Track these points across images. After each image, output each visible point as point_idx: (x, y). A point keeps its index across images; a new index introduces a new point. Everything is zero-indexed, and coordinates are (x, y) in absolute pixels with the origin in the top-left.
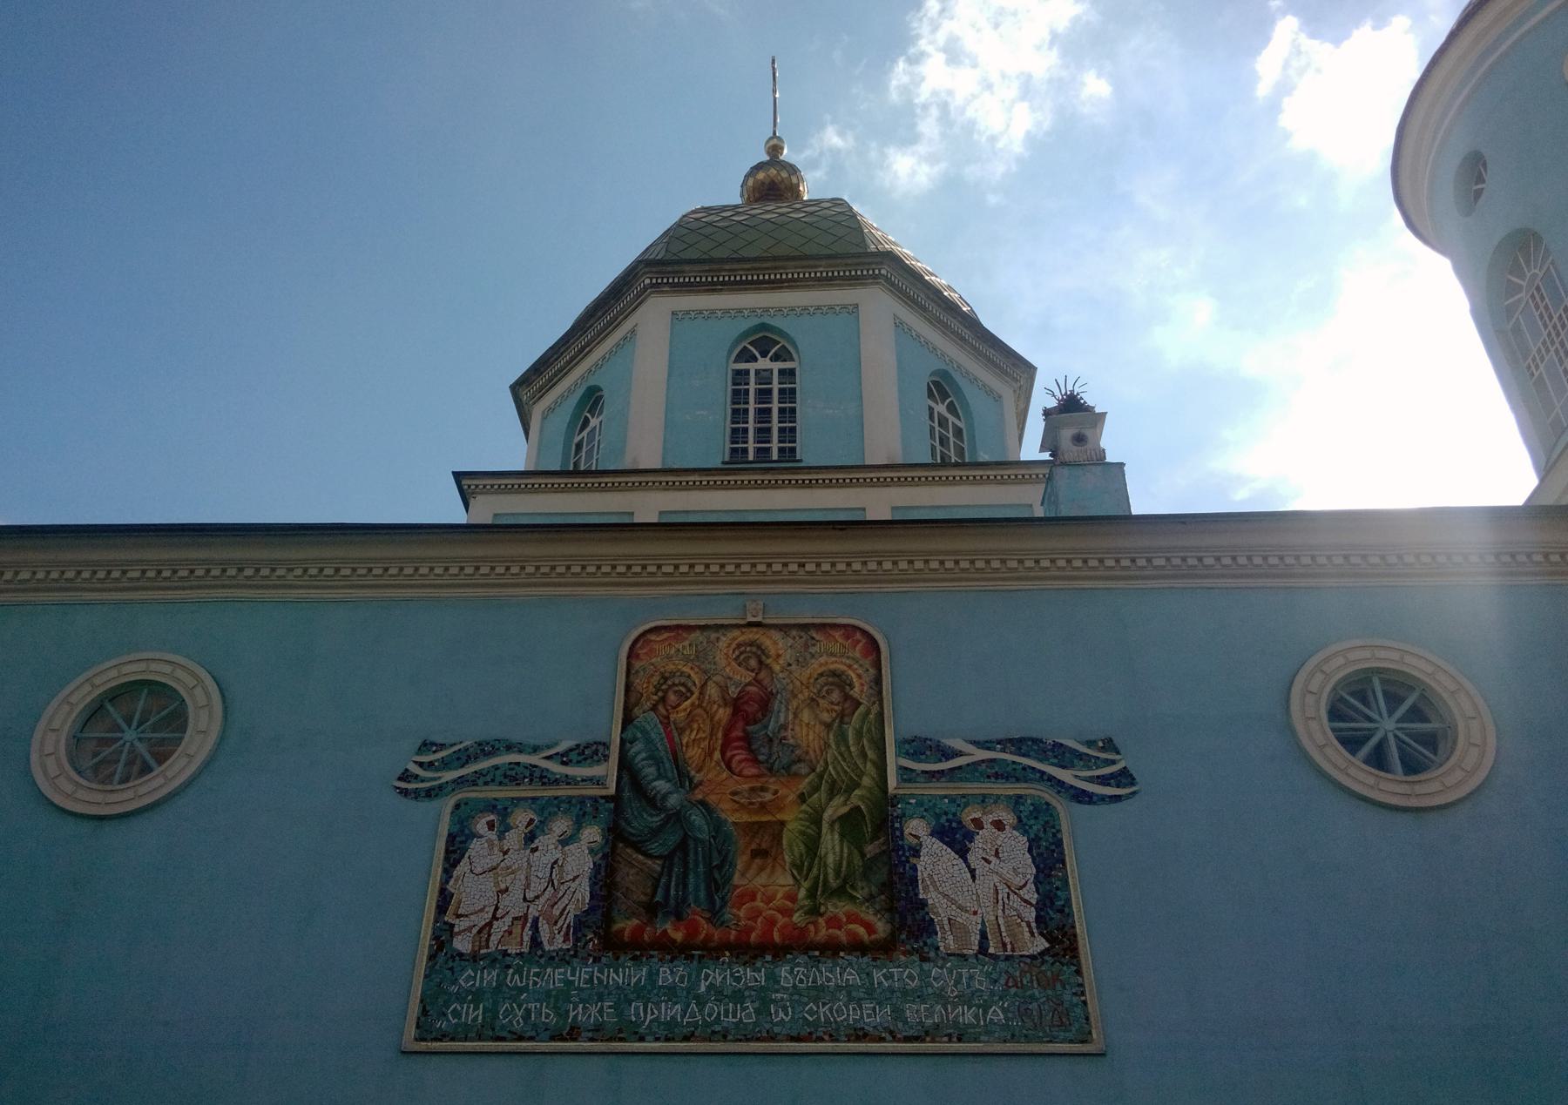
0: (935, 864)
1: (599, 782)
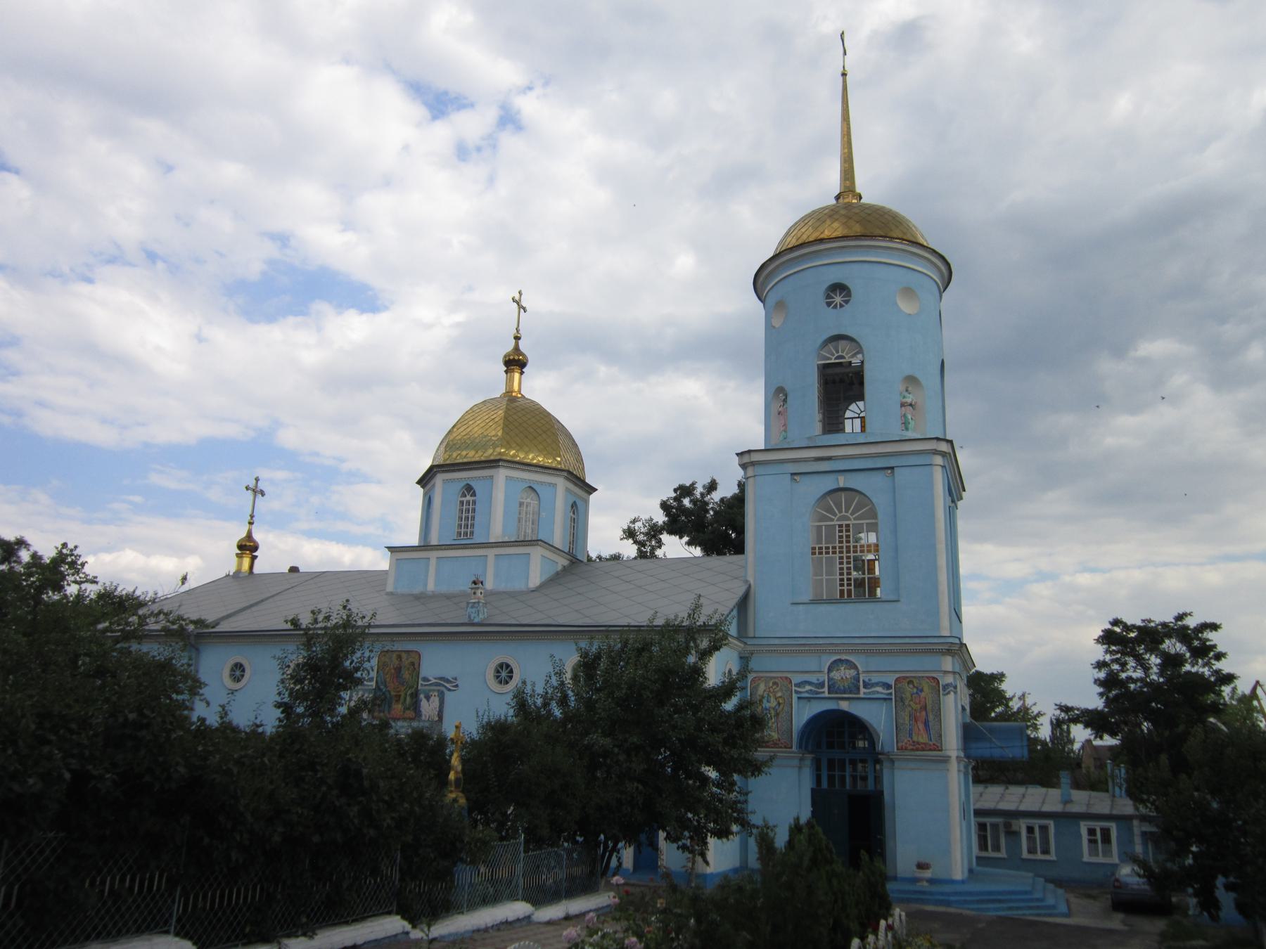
0: (424, 703)
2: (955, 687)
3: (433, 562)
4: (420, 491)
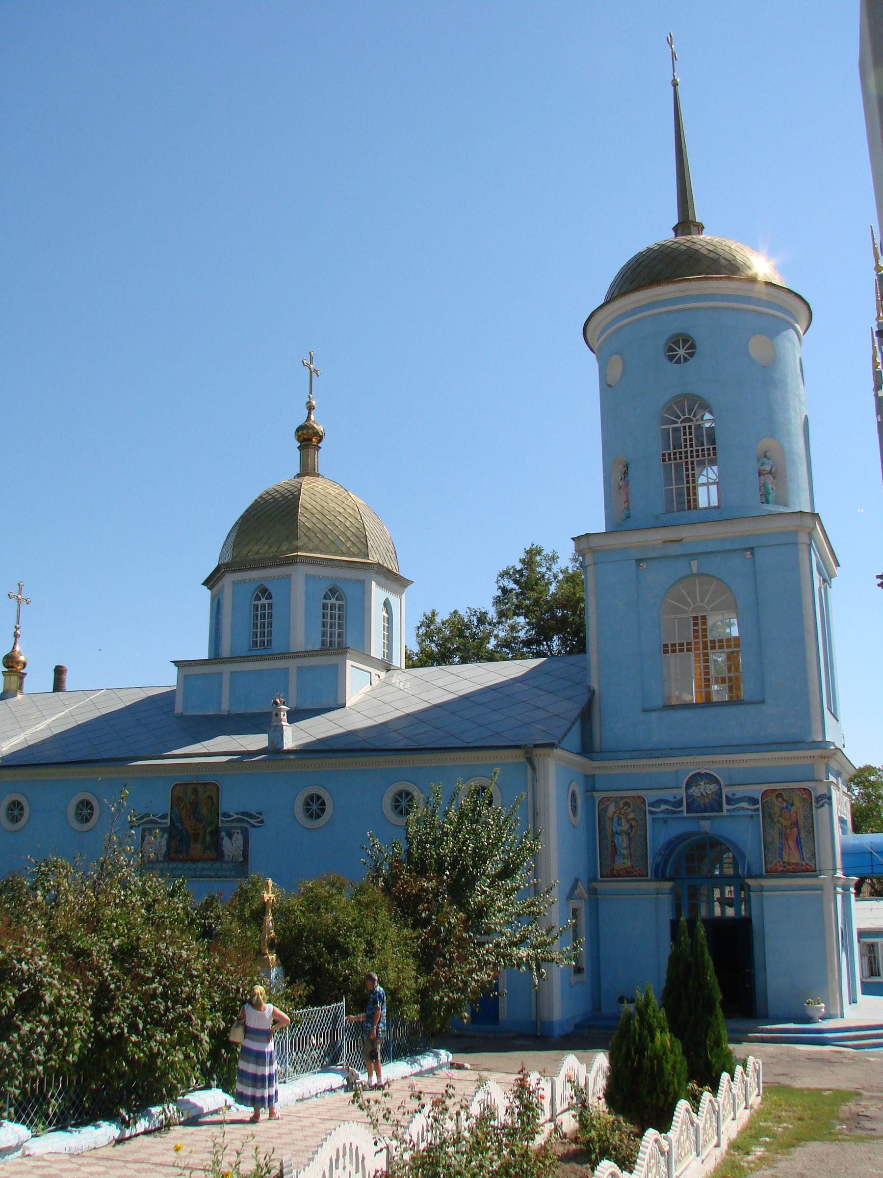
0: (226, 841)
1: (166, 823)
2: (830, 798)
3: (226, 678)
4: (207, 593)
